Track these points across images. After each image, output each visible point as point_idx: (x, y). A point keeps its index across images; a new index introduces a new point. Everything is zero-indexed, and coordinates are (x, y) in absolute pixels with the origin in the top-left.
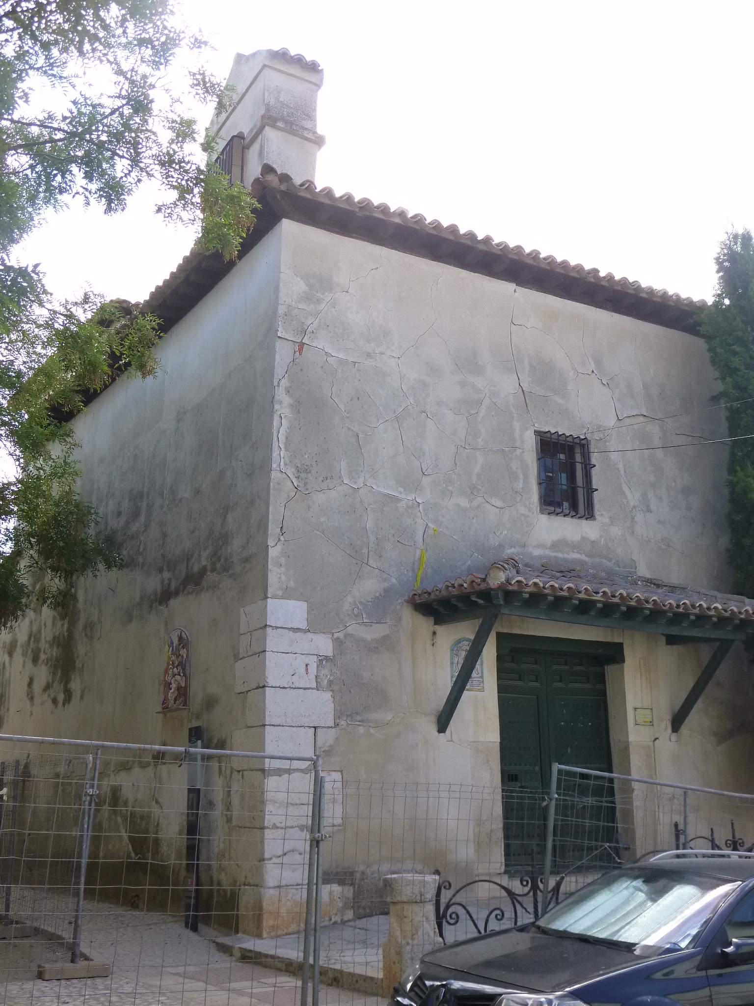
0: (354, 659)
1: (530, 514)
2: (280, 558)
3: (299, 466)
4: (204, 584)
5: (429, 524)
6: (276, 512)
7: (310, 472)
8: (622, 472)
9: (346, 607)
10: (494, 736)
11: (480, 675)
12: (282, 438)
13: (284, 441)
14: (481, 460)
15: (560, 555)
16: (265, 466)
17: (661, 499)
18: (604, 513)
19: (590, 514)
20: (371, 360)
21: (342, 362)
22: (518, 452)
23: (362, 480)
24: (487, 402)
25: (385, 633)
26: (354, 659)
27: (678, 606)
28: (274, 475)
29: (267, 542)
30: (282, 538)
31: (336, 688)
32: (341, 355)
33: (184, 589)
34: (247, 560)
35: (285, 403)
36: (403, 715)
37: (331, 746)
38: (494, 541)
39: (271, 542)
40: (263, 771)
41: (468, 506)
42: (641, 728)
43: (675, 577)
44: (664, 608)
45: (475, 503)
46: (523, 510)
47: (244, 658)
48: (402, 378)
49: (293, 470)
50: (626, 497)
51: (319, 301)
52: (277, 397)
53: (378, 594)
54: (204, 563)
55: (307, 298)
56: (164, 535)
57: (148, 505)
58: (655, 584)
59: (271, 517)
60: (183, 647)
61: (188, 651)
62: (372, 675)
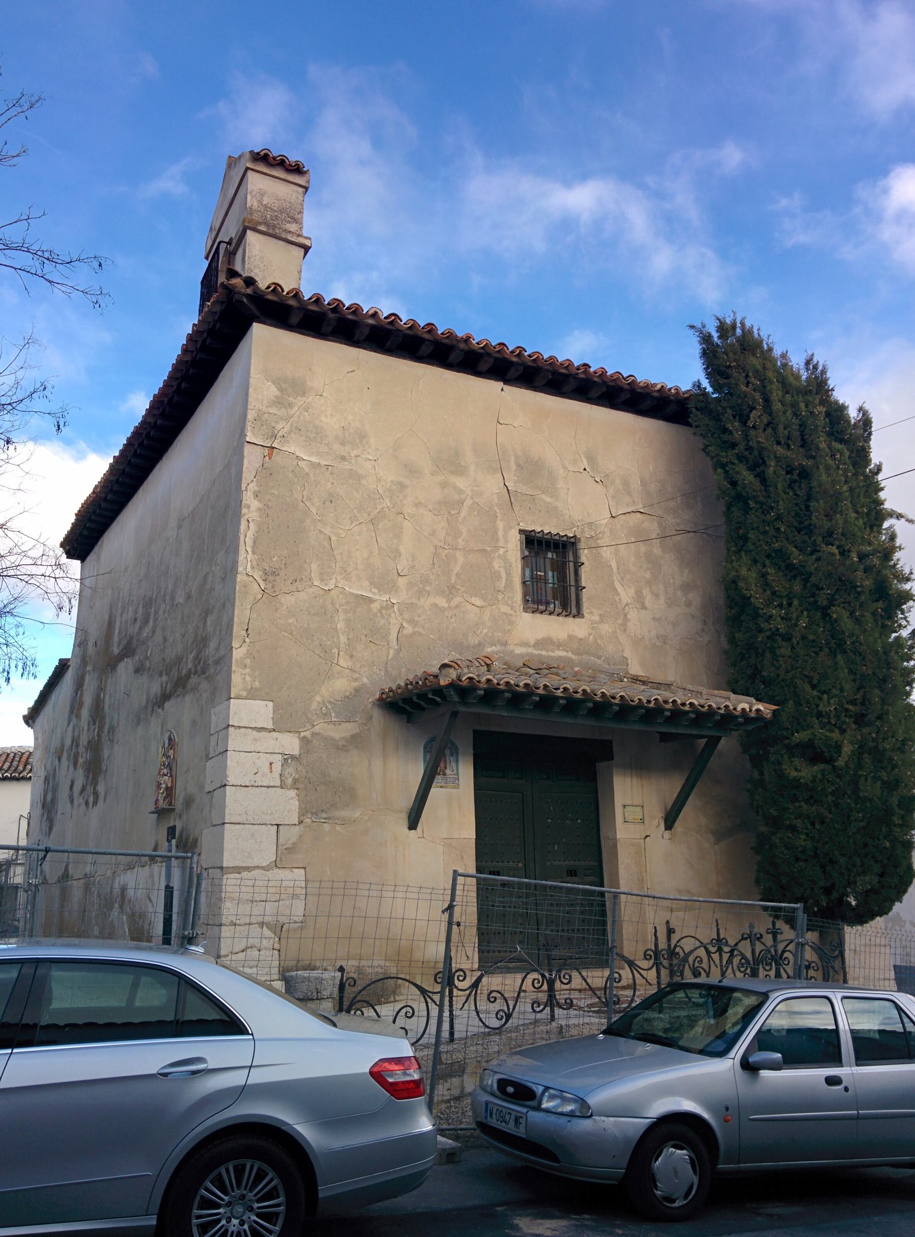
0: (321, 757)
1: (512, 612)
2: (244, 658)
3: (267, 568)
4: (189, 686)
5: (405, 624)
6: (242, 613)
7: (279, 574)
8: (615, 570)
9: (314, 706)
10: (469, 832)
11: (455, 772)
12: (249, 541)
13: (252, 545)
14: (461, 560)
15: (544, 653)
16: (231, 571)
17: (657, 596)
18: (594, 611)
19: (579, 614)
20: (345, 463)
21: (315, 466)
22: (501, 551)
23: (333, 581)
24: (468, 502)
25: (354, 732)
26: (321, 757)
27: (649, 702)
28: (239, 578)
29: (231, 643)
30: (247, 640)
31: (301, 786)
32: (314, 459)
33: (175, 692)
34: (217, 662)
35: (253, 508)
36: (371, 812)
37: (294, 844)
38: (474, 640)
39: (235, 644)
40: (222, 868)
41: (446, 606)
42: (631, 826)
43: (671, 675)
44: (633, 704)
45: (454, 603)
46: (505, 609)
47: (212, 757)
48: (379, 480)
49: (261, 573)
50: (618, 594)
51: (290, 405)
52: (244, 502)
53: (348, 694)
54: (190, 667)
55: (278, 402)
56: (165, 640)
57: (155, 611)
58: (640, 681)
59: (236, 619)
60: (171, 749)
61: (174, 751)
62: (340, 773)
